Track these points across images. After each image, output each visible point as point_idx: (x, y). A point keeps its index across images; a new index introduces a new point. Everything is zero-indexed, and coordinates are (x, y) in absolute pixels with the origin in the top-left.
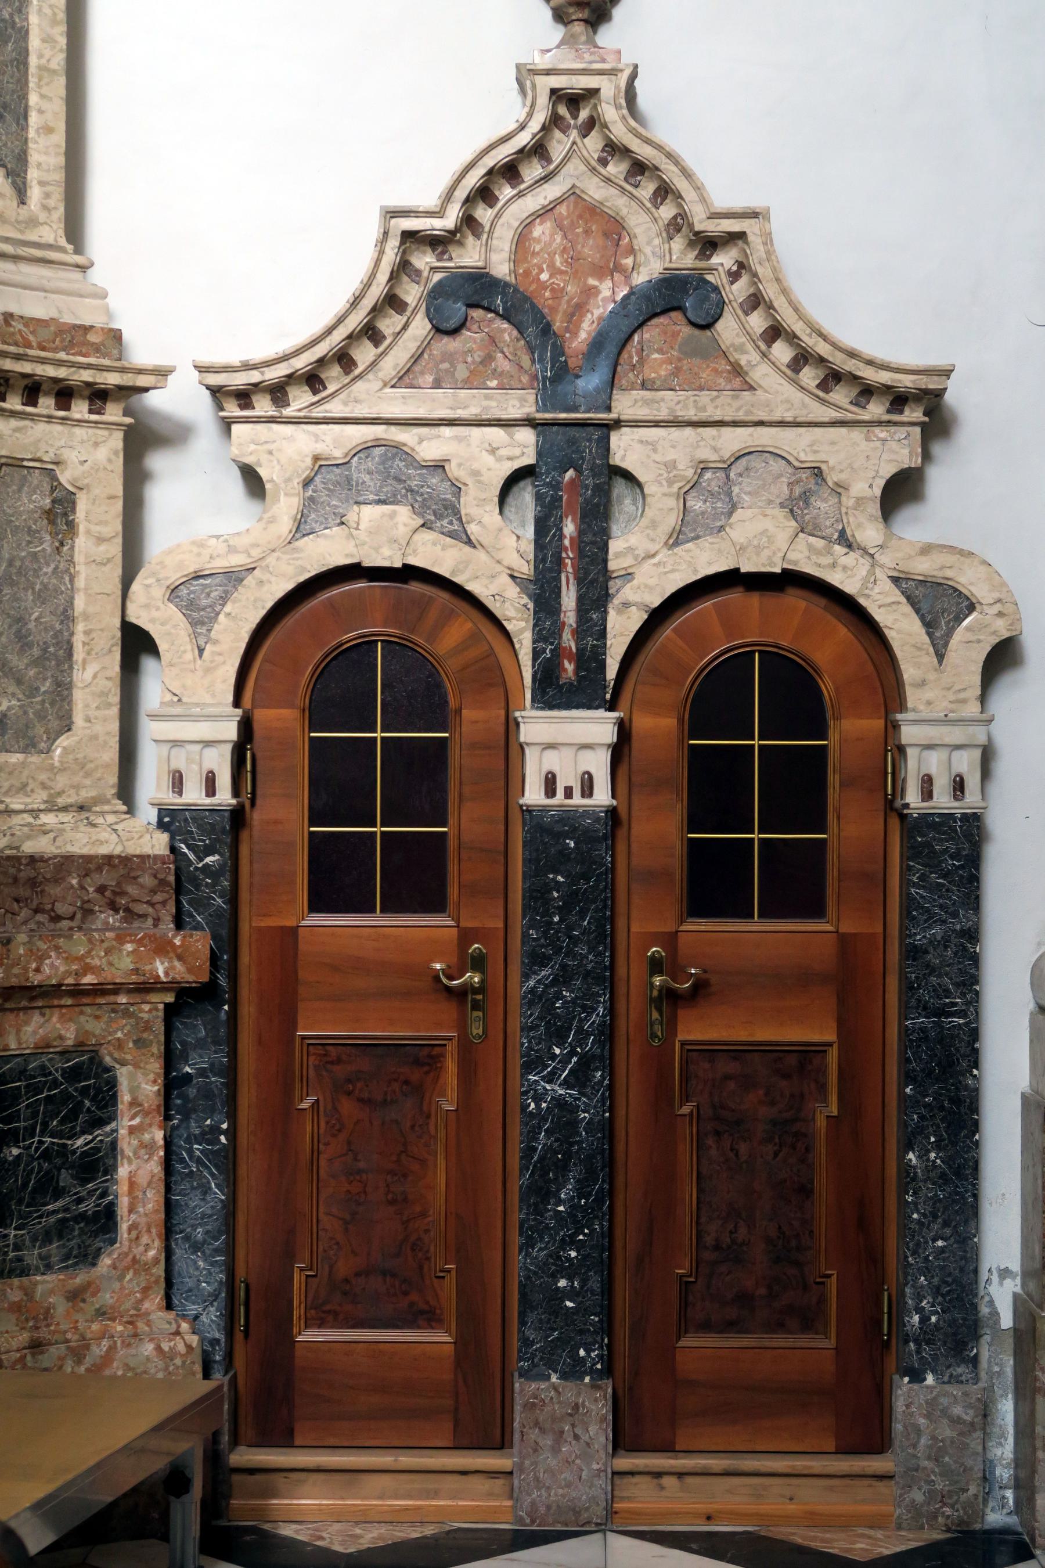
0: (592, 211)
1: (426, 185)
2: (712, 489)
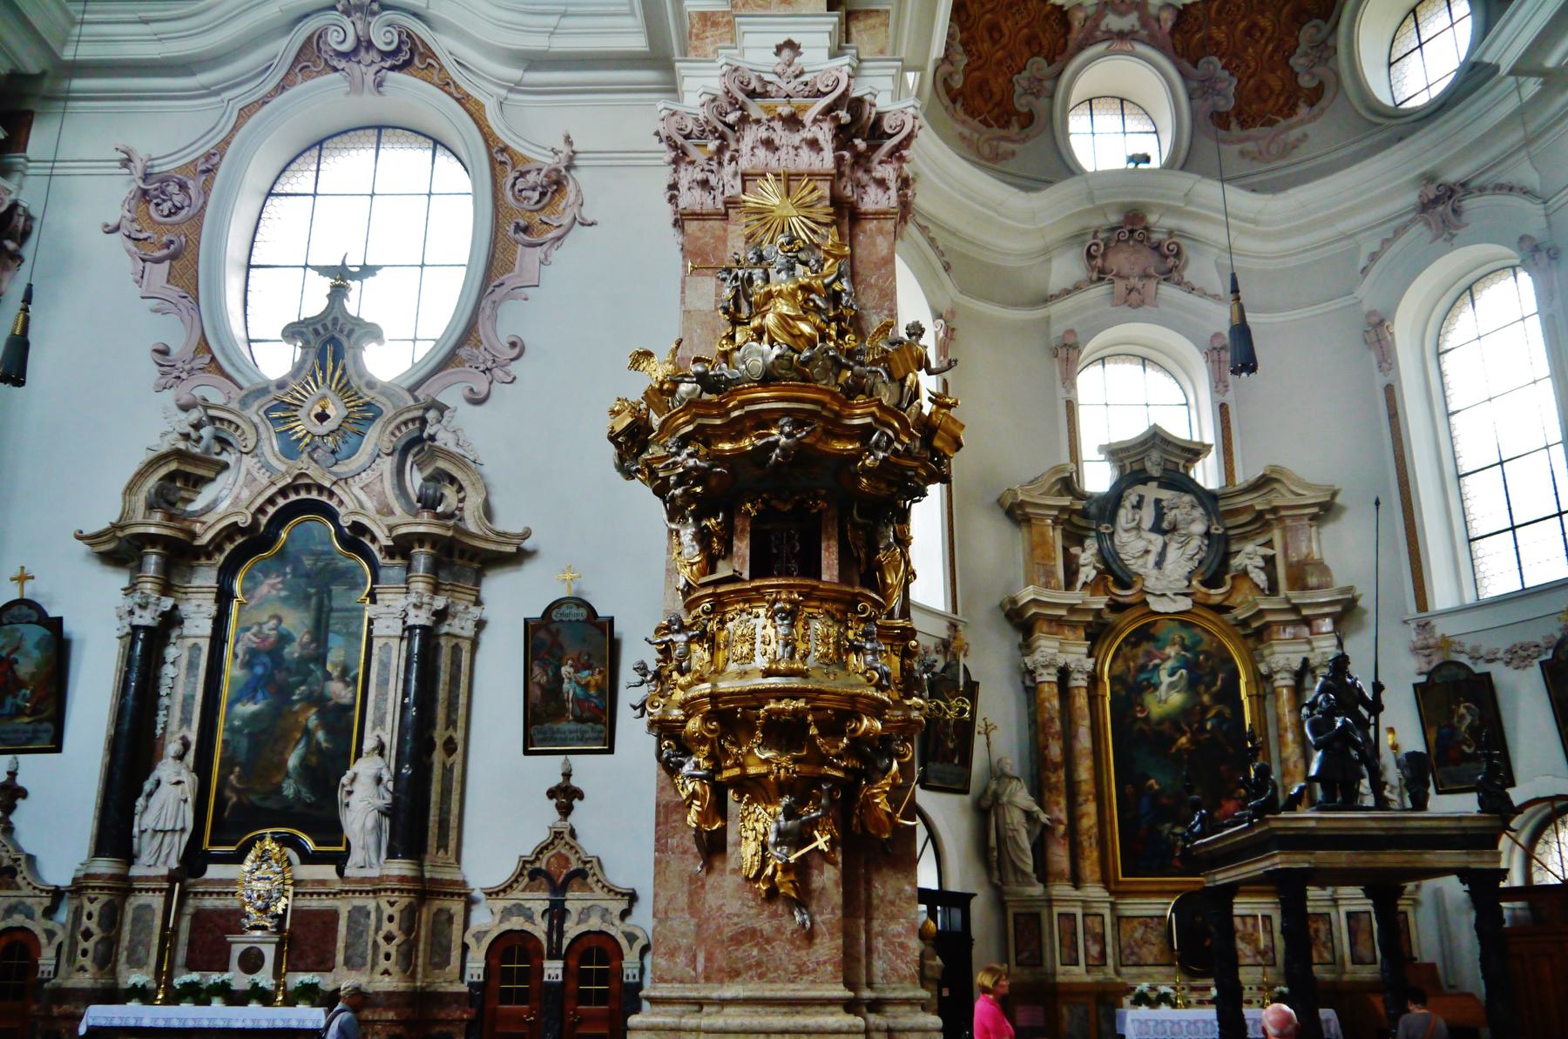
1: (528, 850)
2: (585, 914)
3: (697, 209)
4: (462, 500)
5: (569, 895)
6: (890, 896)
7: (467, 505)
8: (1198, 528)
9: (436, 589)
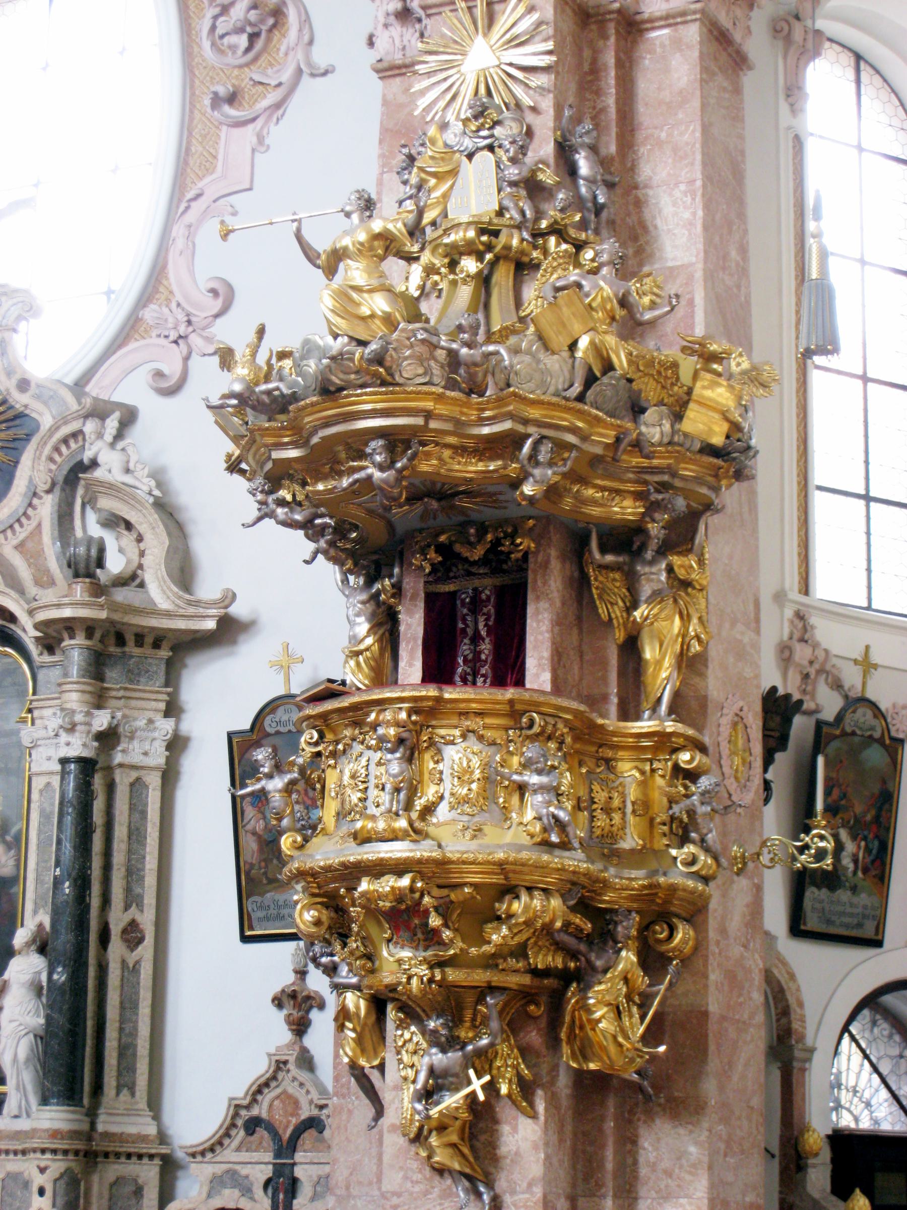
0: (290, 1097)
1: (240, 1089)
3: (398, 58)
4: (142, 554)
5: (299, 1156)
6: (666, 1164)
7: (147, 561)
9: (99, 700)
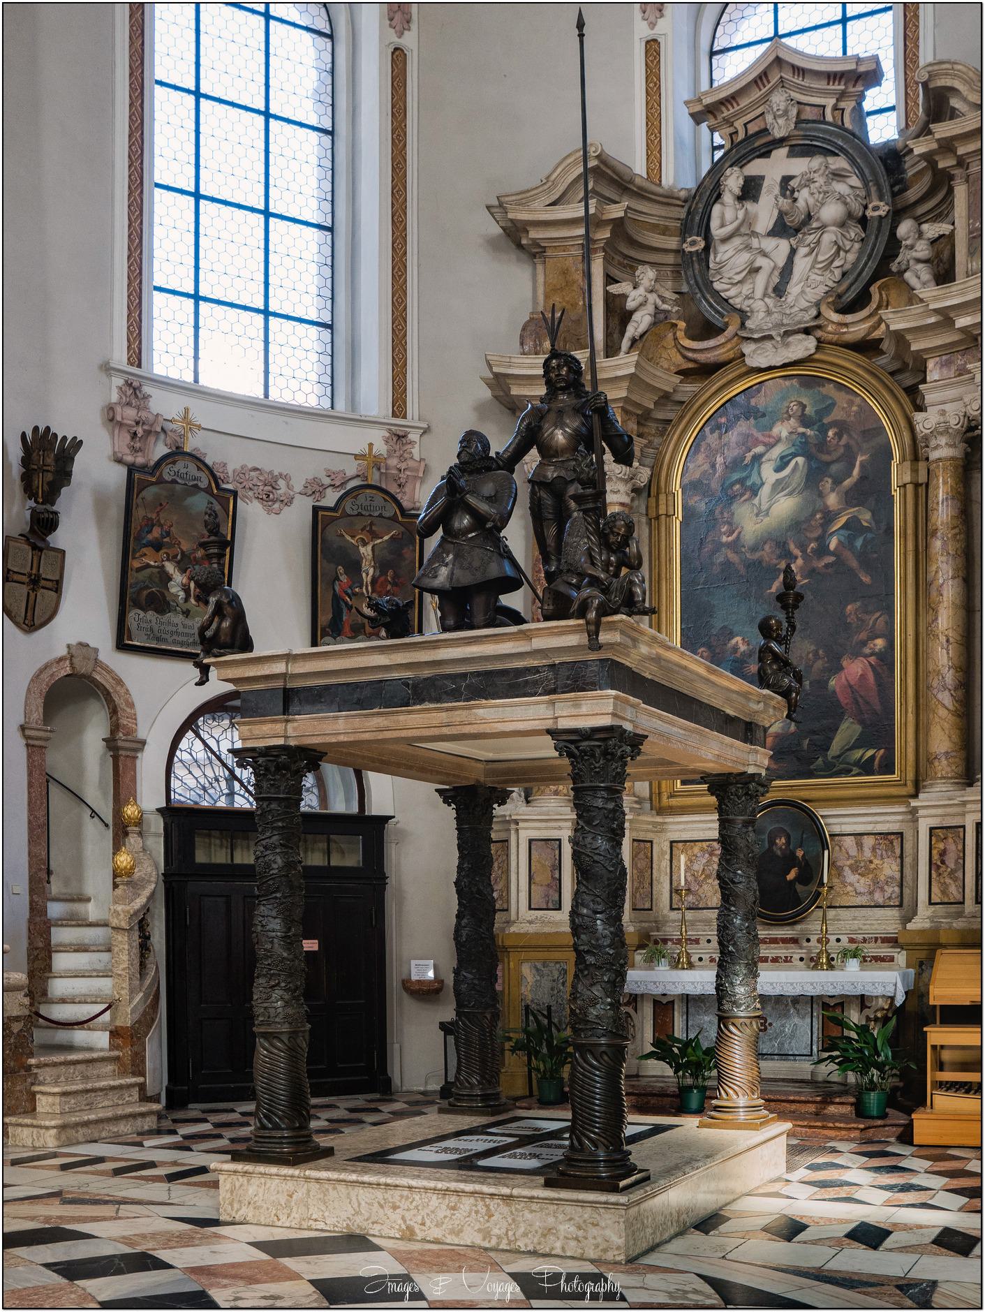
8: (831, 212)
